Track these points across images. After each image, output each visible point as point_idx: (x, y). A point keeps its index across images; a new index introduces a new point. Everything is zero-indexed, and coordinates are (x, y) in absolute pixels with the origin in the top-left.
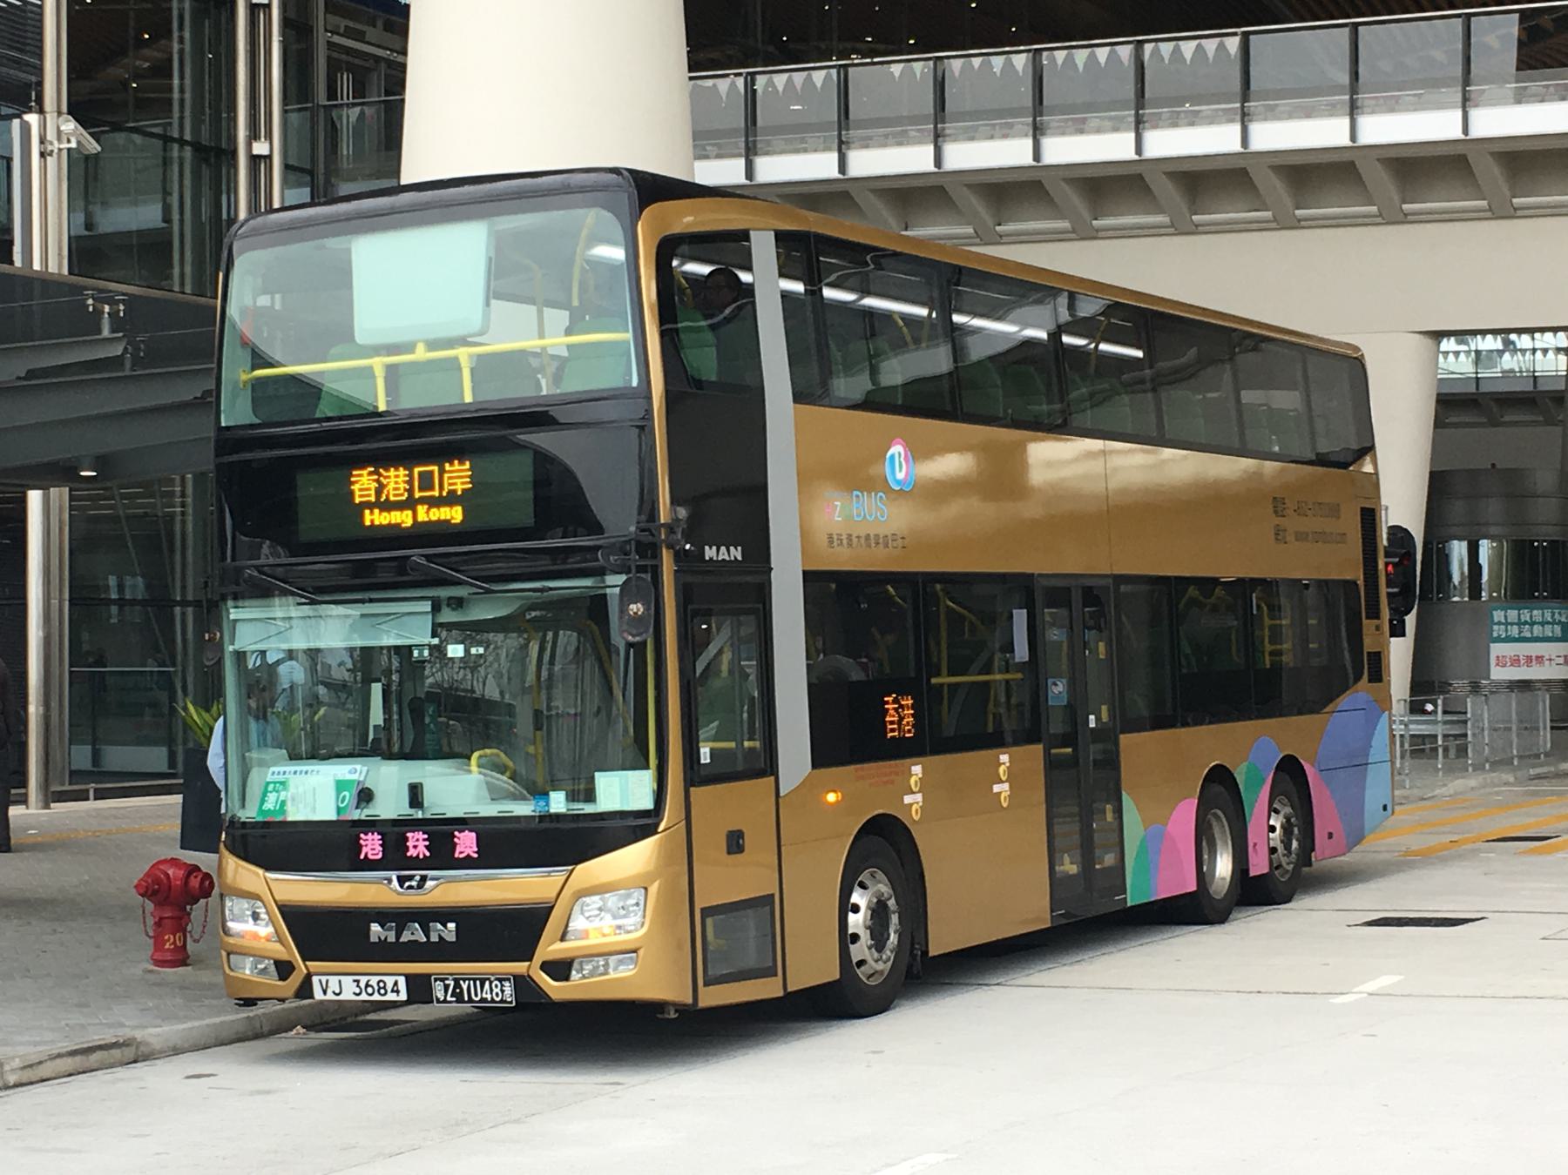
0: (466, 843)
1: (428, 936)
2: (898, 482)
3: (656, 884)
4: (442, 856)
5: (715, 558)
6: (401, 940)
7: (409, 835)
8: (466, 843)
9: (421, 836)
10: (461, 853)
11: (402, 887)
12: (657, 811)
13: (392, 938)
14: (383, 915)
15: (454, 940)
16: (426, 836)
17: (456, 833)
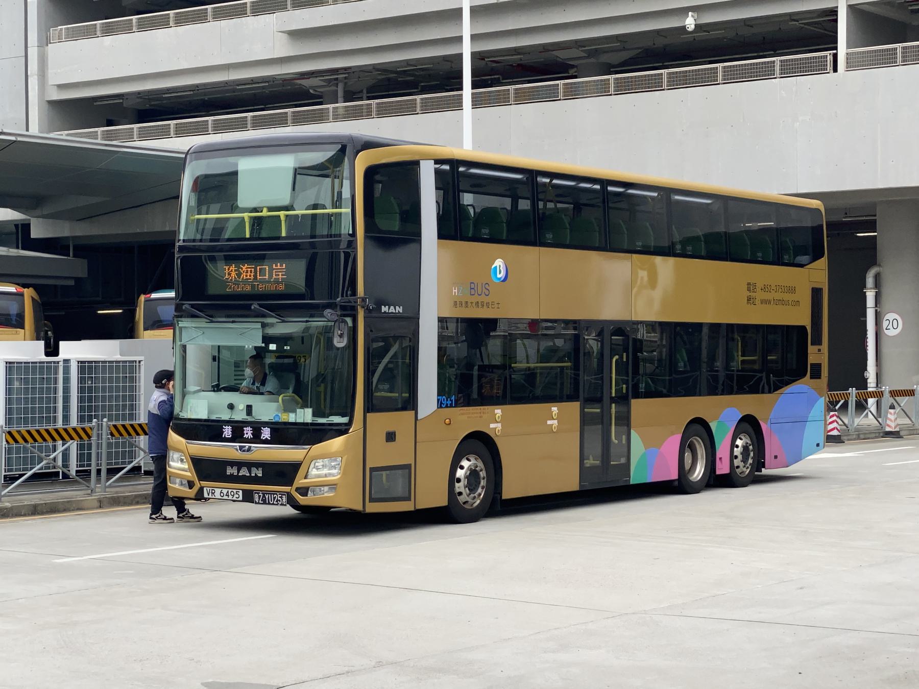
0: (266, 433)
1: (250, 473)
3: (346, 456)
5: (387, 311)
6: (239, 474)
7: (245, 428)
8: (266, 433)
9: (249, 429)
10: (263, 437)
11: (240, 450)
14: (232, 463)
15: (261, 475)
16: (251, 429)
17: (262, 428)
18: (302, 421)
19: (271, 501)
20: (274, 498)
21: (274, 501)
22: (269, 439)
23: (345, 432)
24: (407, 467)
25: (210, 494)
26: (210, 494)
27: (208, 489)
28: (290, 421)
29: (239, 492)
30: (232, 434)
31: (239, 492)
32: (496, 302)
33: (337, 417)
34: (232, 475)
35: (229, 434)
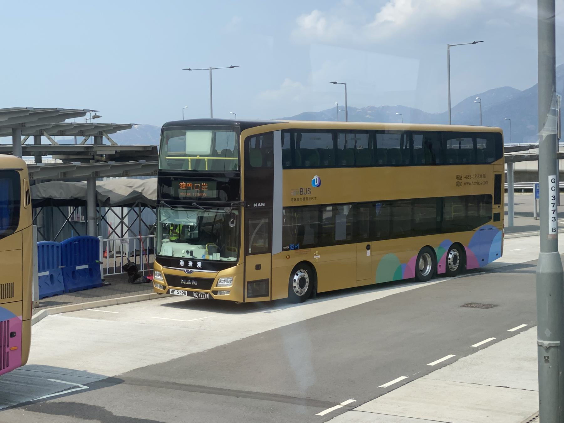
0: (199, 265)
1: (191, 283)
4: (195, 266)
5: (257, 206)
7: (189, 262)
8: (199, 265)
9: (191, 262)
13: (185, 283)
18: (215, 259)
22: (201, 267)
27: (172, 290)
28: (210, 259)
33: (232, 258)
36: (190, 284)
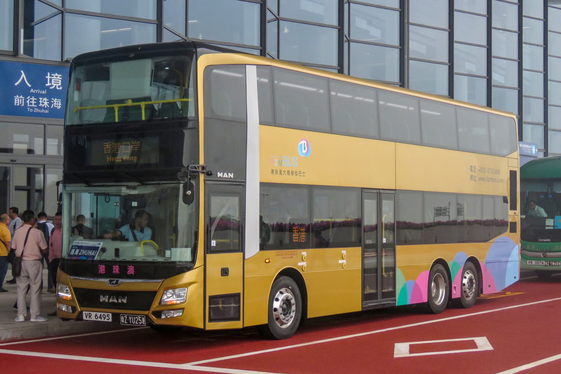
0: (131, 270)
1: (118, 300)
2: (303, 154)
4: (123, 274)
5: (222, 177)
7: (114, 266)
8: (131, 270)
9: (117, 267)
10: (129, 273)
12: (194, 261)
13: (107, 301)
16: (118, 267)
17: (128, 266)
19: (134, 322)
20: (136, 320)
21: (136, 322)
22: (133, 274)
23: (189, 269)
24: (238, 295)
25: (88, 317)
26: (88, 317)
27: (87, 312)
29: (109, 315)
30: (105, 271)
31: (109, 315)
32: (302, 172)
34: (104, 302)
35: (103, 271)
36: (115, 301)
